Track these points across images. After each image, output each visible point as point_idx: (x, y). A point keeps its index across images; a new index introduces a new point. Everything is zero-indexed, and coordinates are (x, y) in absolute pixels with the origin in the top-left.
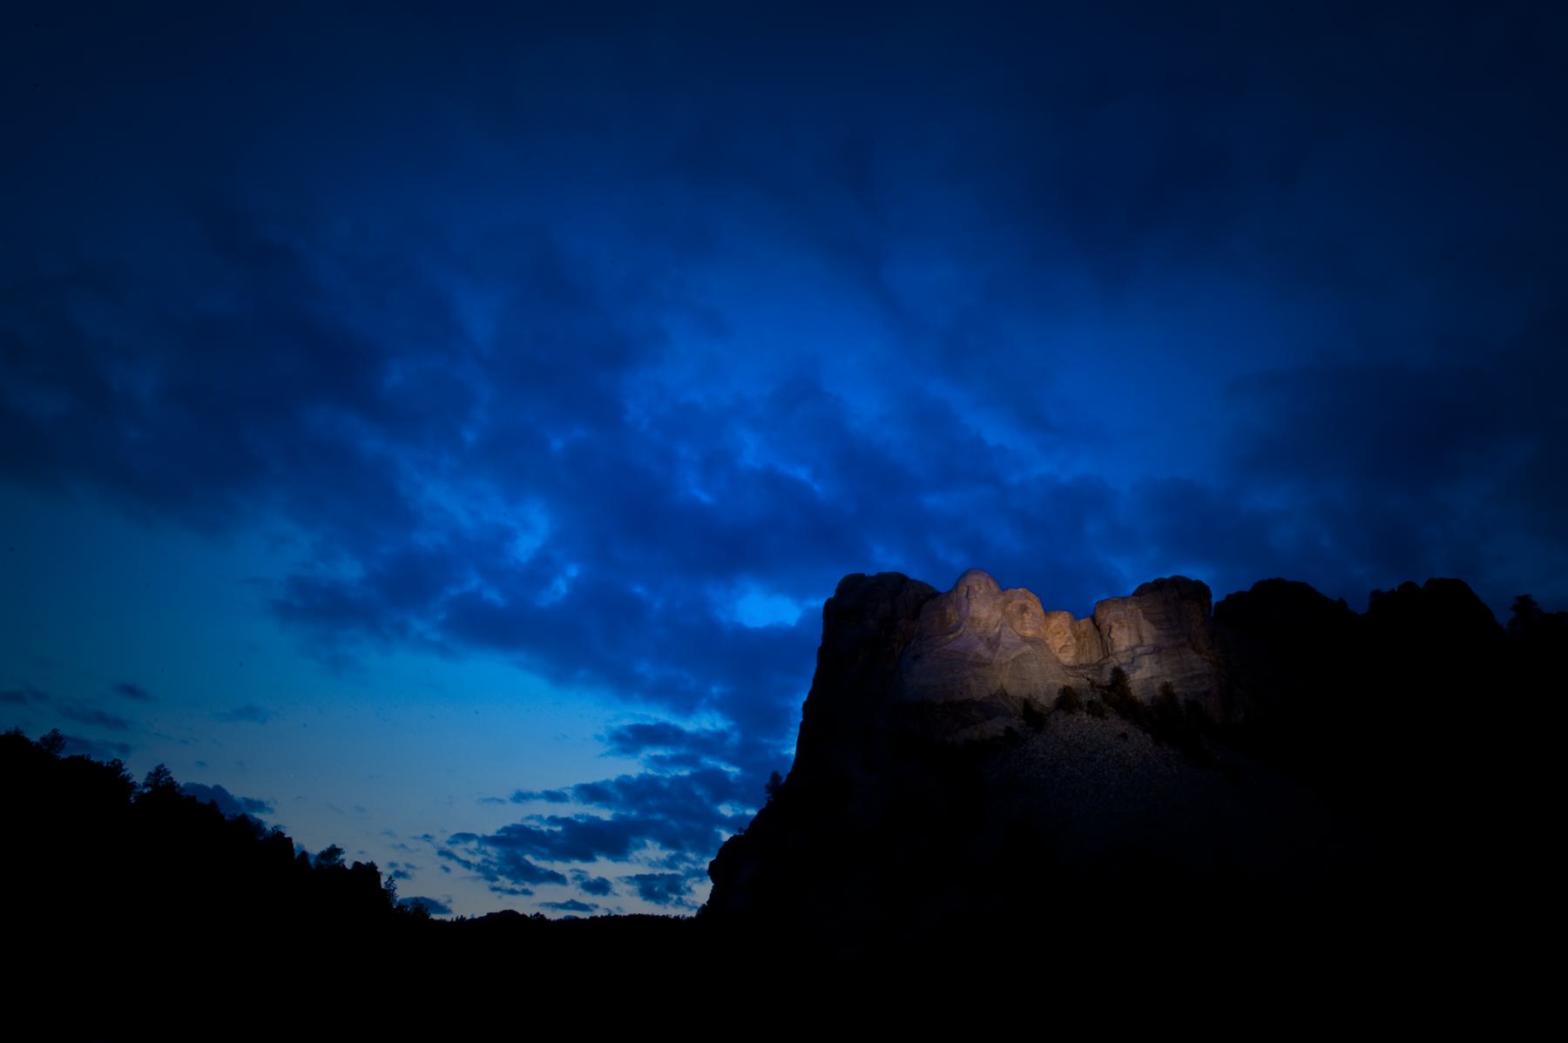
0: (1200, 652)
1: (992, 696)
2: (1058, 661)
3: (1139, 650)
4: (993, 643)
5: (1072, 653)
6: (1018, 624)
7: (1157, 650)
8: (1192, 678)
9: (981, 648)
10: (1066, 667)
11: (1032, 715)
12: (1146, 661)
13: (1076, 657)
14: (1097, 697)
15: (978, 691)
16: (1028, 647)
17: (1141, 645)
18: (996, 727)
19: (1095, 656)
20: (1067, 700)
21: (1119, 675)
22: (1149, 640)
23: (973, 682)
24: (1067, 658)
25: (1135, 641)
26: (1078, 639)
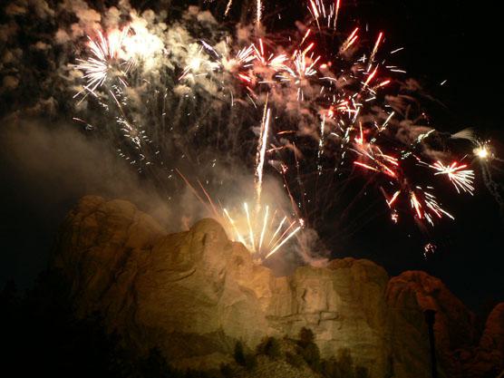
0: (372, 326)
1: (213, 334)
3: (325, 315)
4: (219, 287)
7: (338, 318)
8: (363, 347)
9: (209, 291)
11: (240, 355)
12: (330, 324)
14: (291, 349)
15: (201, 328)
16: (244, 297)
17: (327, 310)
18: (216, 361)
19: (285, 310)
20: (269, 347)
21: (307, 335)
22: (333, 308)
23: (199, 319)
25: (322, 307)
26: (273, 292)
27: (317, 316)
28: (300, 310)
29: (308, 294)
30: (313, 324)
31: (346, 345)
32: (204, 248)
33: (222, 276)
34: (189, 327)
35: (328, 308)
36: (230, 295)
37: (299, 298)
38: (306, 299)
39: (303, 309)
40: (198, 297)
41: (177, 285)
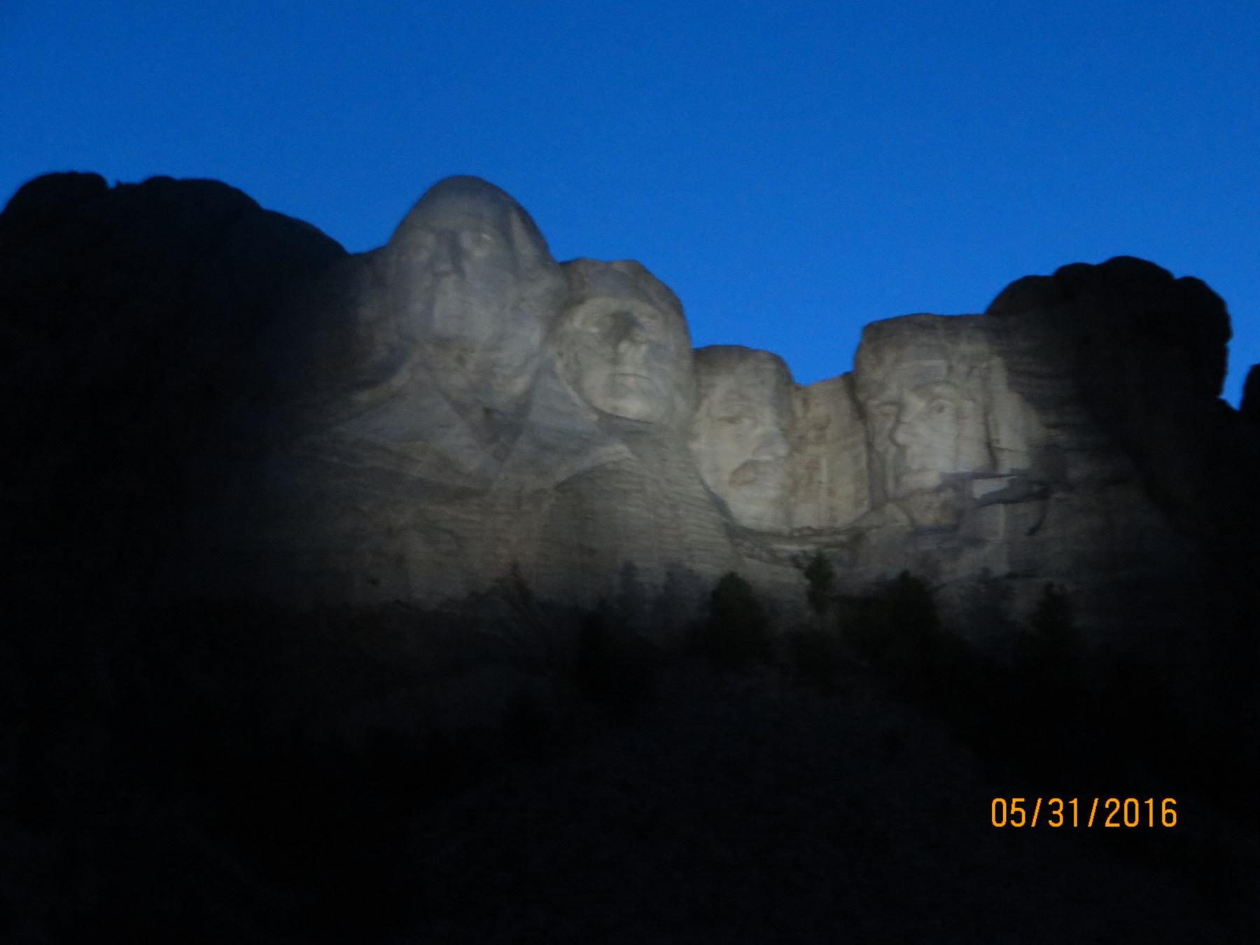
2: (719, 505)
5: (770, 489)
6: (596, 379)
17: (991, 471)
22: (1016, 457)
24: (753, 507)
25: (972, 459)
26: (796, 447)
28: (890, 485)
30: (936, 530)
37: (881, 444)
39: (897, 479)
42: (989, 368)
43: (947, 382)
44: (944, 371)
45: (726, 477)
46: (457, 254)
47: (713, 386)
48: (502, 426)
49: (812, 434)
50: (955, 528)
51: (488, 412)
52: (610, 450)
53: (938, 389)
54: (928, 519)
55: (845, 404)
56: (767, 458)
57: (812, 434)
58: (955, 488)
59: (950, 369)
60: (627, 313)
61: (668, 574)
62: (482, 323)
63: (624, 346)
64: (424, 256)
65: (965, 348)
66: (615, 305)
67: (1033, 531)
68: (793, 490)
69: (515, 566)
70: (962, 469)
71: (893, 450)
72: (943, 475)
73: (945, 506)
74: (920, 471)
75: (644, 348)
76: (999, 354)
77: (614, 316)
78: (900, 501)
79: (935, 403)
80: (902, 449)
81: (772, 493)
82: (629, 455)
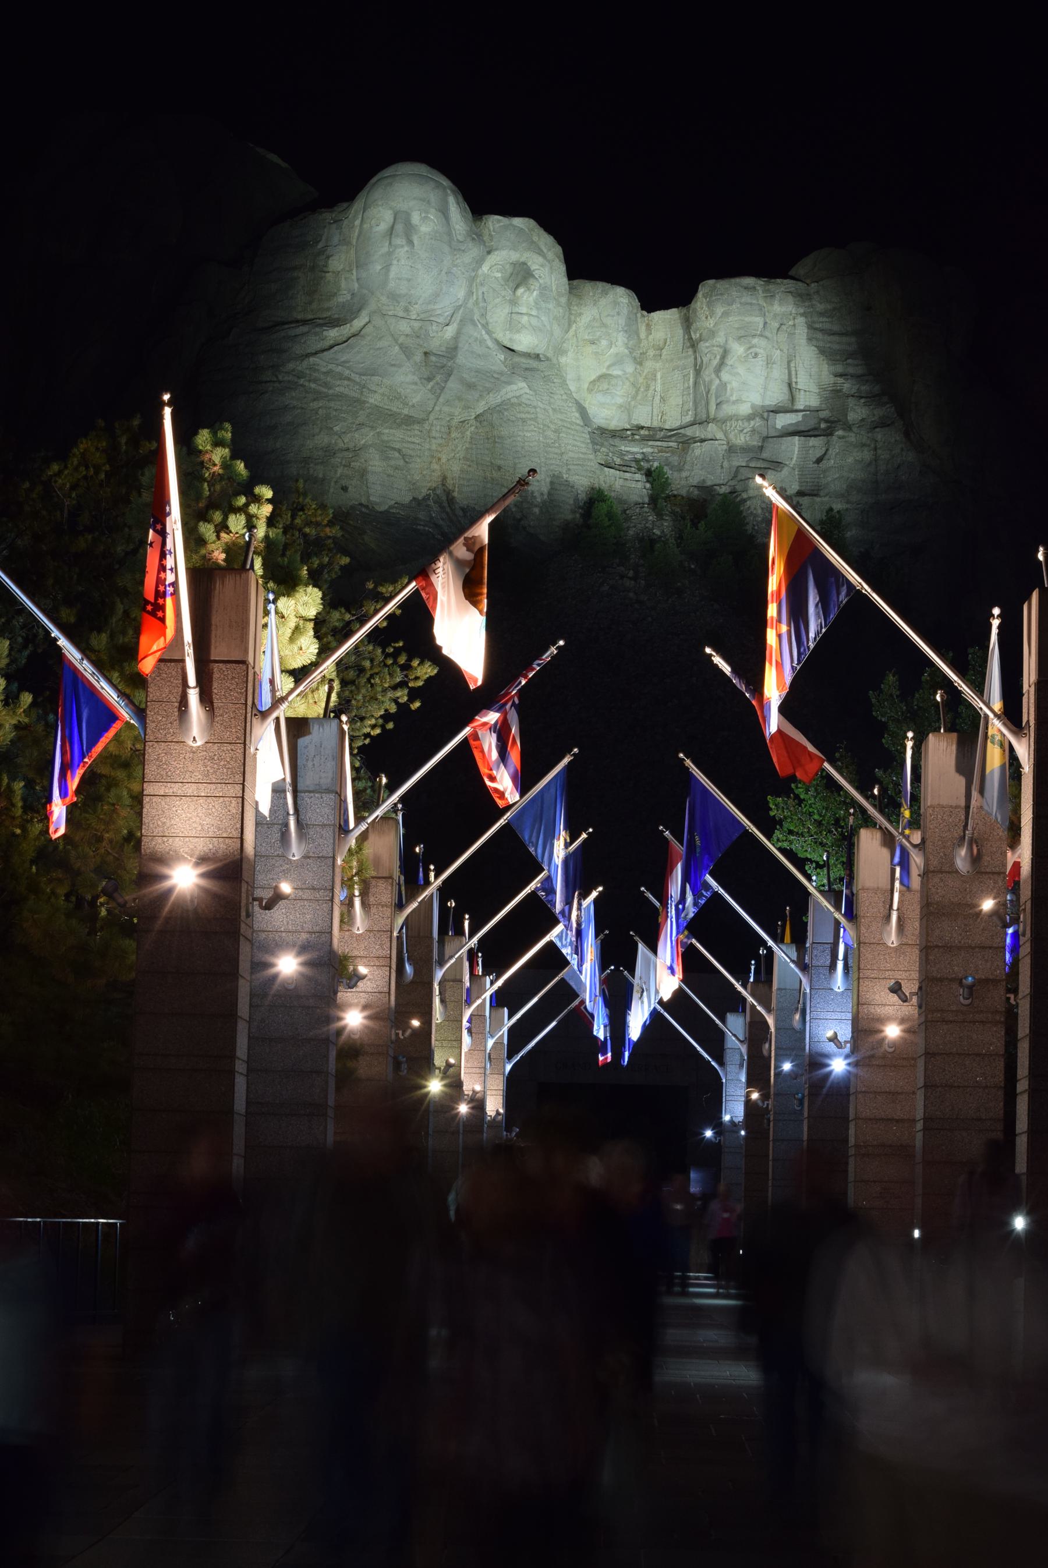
5: (620, 394)
6: (498, 315)
10: (604, 435)
13: (627, 409)
22: (809, 397)
23: (375, 464)
24: (607, 411)
25: (776, 395)
26: (639, 362)
27: (757, 423)
29: (730, 361)
30: (746, 449)
31: (837, 506)
32: (390, 254)
33: (450, 332)
34: (345, 489)
35: (793, 399)
36: (471, 386)
37: (708, 374)
38: (725, 376)
40: (373, 400)
41: (313, 368)
42: (794, 325)
43: (761, 336)
44: (761, 326)
45: (586, 386)
46: (409, 229)
47: (580, 314)
48: (439, 365)
49: (651, 353)
50: (761, 448)
51: (426, 354)
52: (514, 387)
53: (755, 341)
54: (741, 440)
55: (680, 332)
56: (616, 372)
57: (651, 353)
58: (762, 417)
59: (765, 323)
60: (524, 264)
61: (552, 483)
62: (425, 284)
63: (520, 291)
64: (383, 227)
65: (777, 308)
66: (515, 256)
67: (819, 461)
68: (634, 398)
69: (445, 478)
70: (767, 403)
71: (717, 382)
72: (753, 406)
73: (753, 431)
74: (734, 402)
75: (535, 293)
76: (802, 315)
77: (514, 264)
78: (722, 422)
79: (753, 350)
80: (723, 386)
81: (620, 401)
82: (528, 391)
